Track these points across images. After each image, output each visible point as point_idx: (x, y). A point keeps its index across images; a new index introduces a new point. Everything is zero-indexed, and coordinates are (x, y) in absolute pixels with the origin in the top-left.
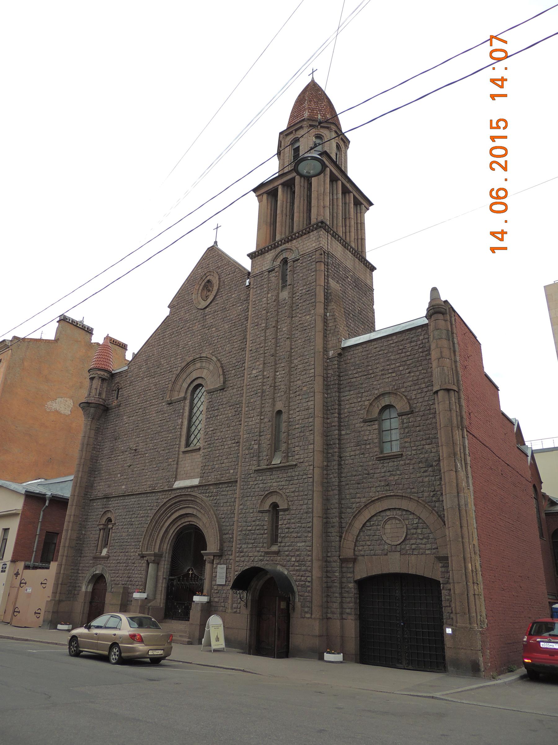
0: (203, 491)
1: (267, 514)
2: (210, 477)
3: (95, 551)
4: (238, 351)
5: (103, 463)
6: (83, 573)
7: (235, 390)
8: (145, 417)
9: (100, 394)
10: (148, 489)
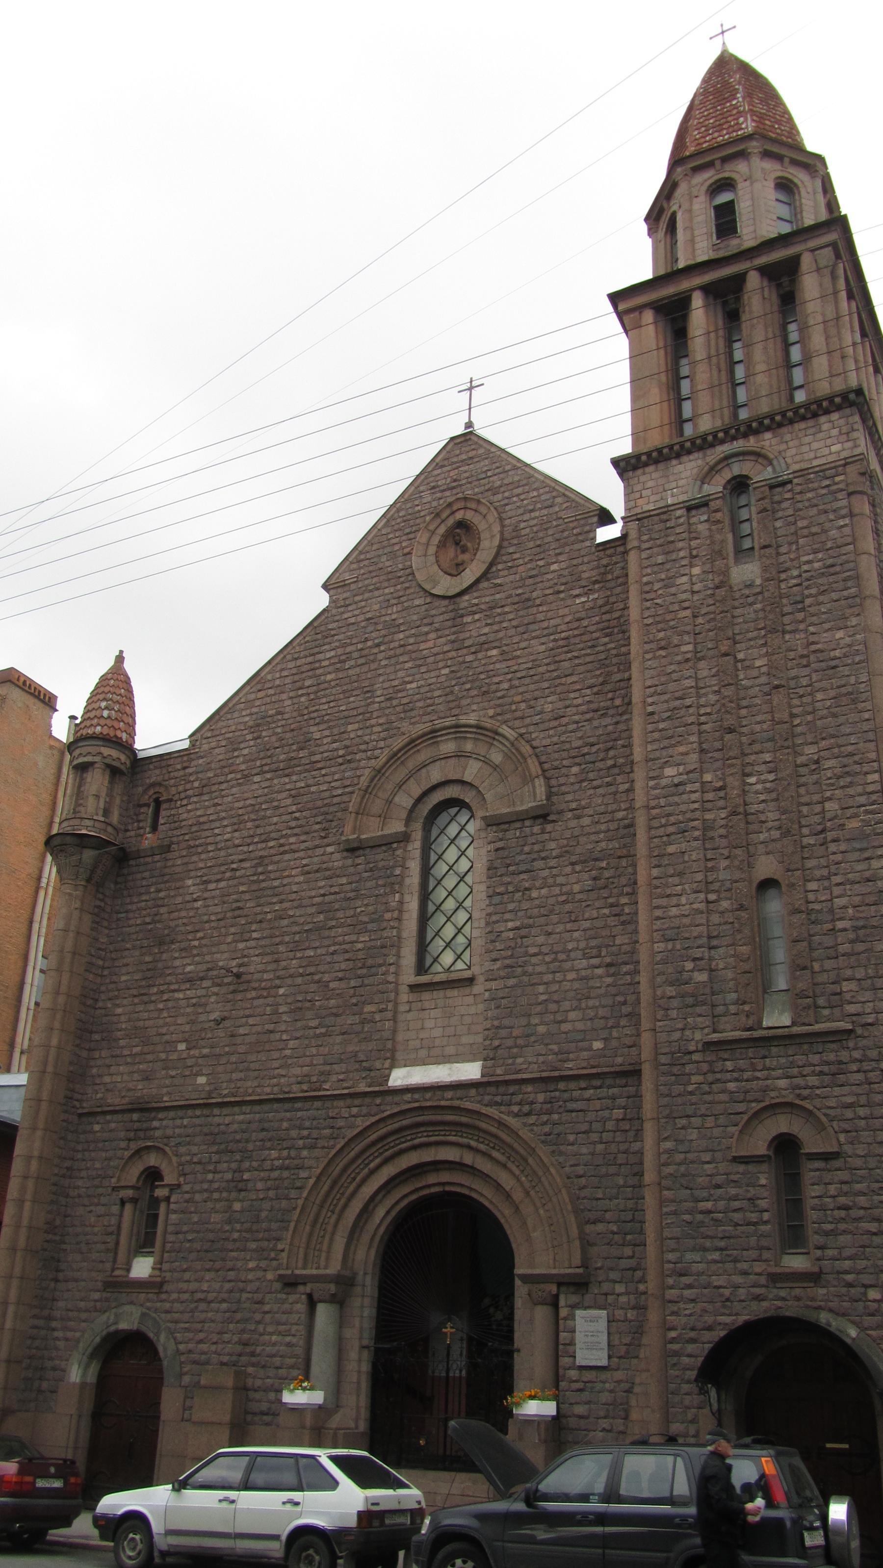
0: (498, 1099)
1: (765, 1167)
2: (519, 1060)
3: (108, 1266)
4: (588, 716)
5: (119, 1011)
6: (65, 1328)
7: (586, 821)
8: (264, 885)
9: (106, 812)
10: (295, 1088)
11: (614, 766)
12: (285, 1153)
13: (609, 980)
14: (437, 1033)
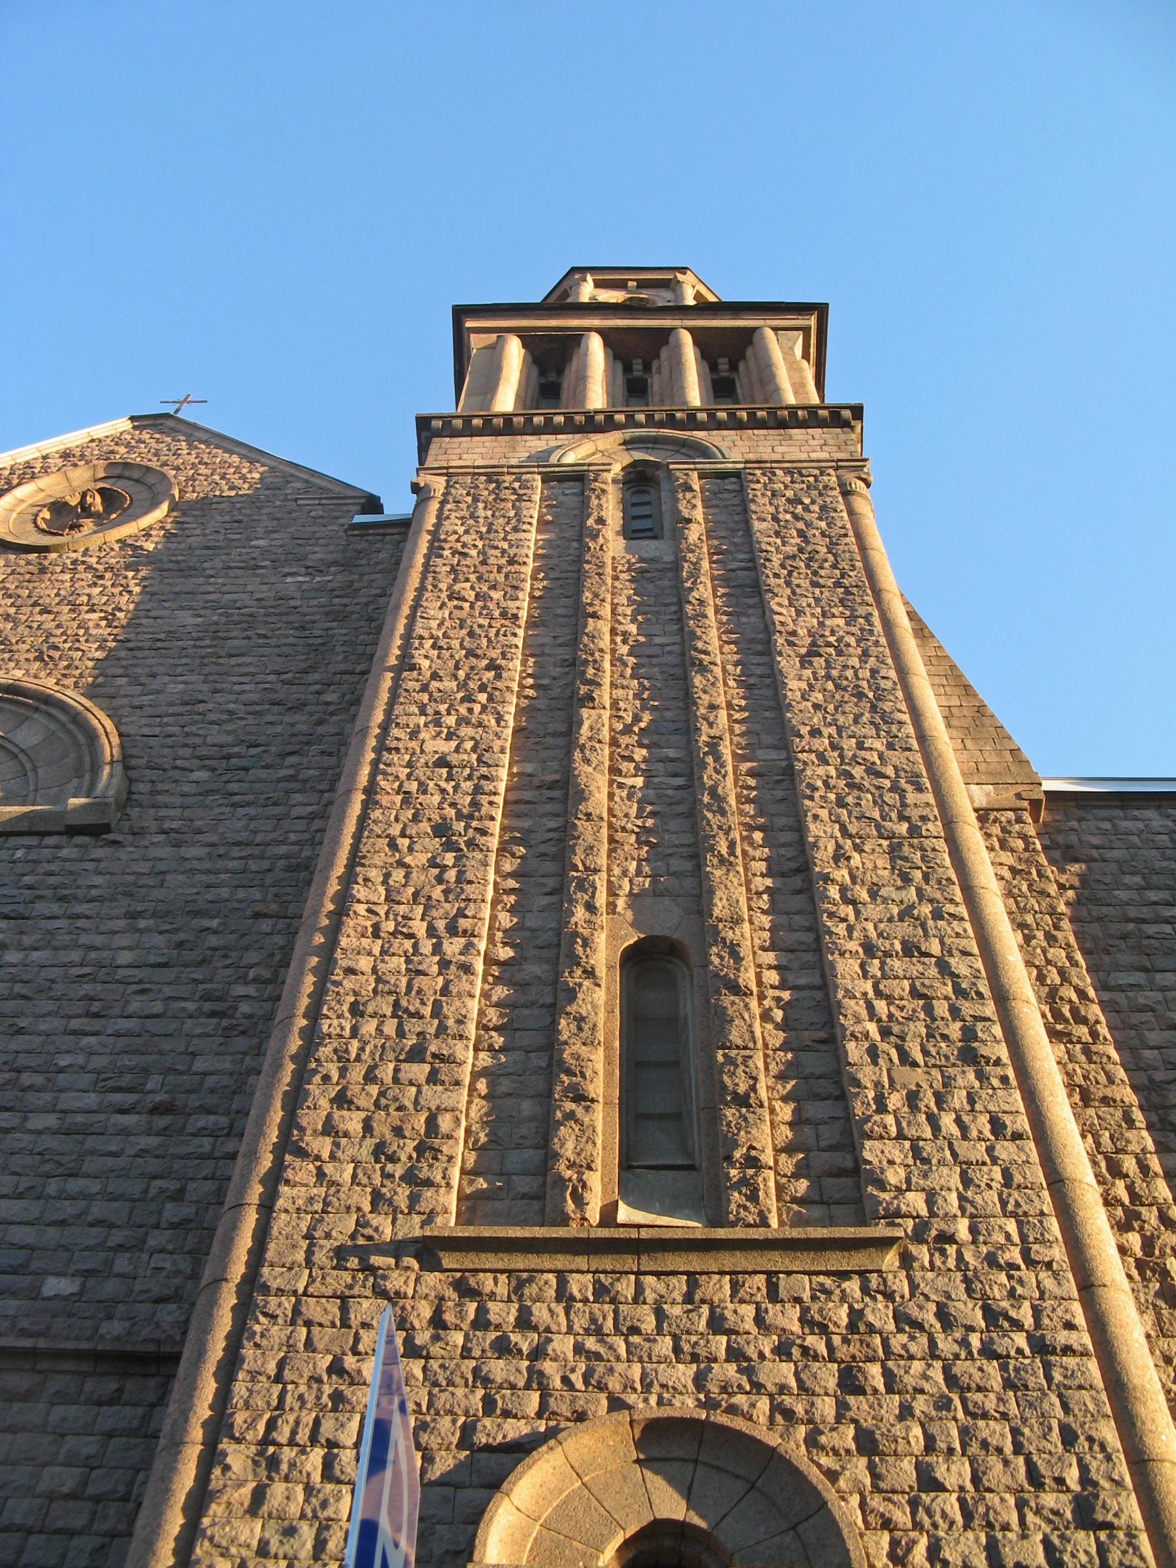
11: (293, 778)
13: (153, 1141)
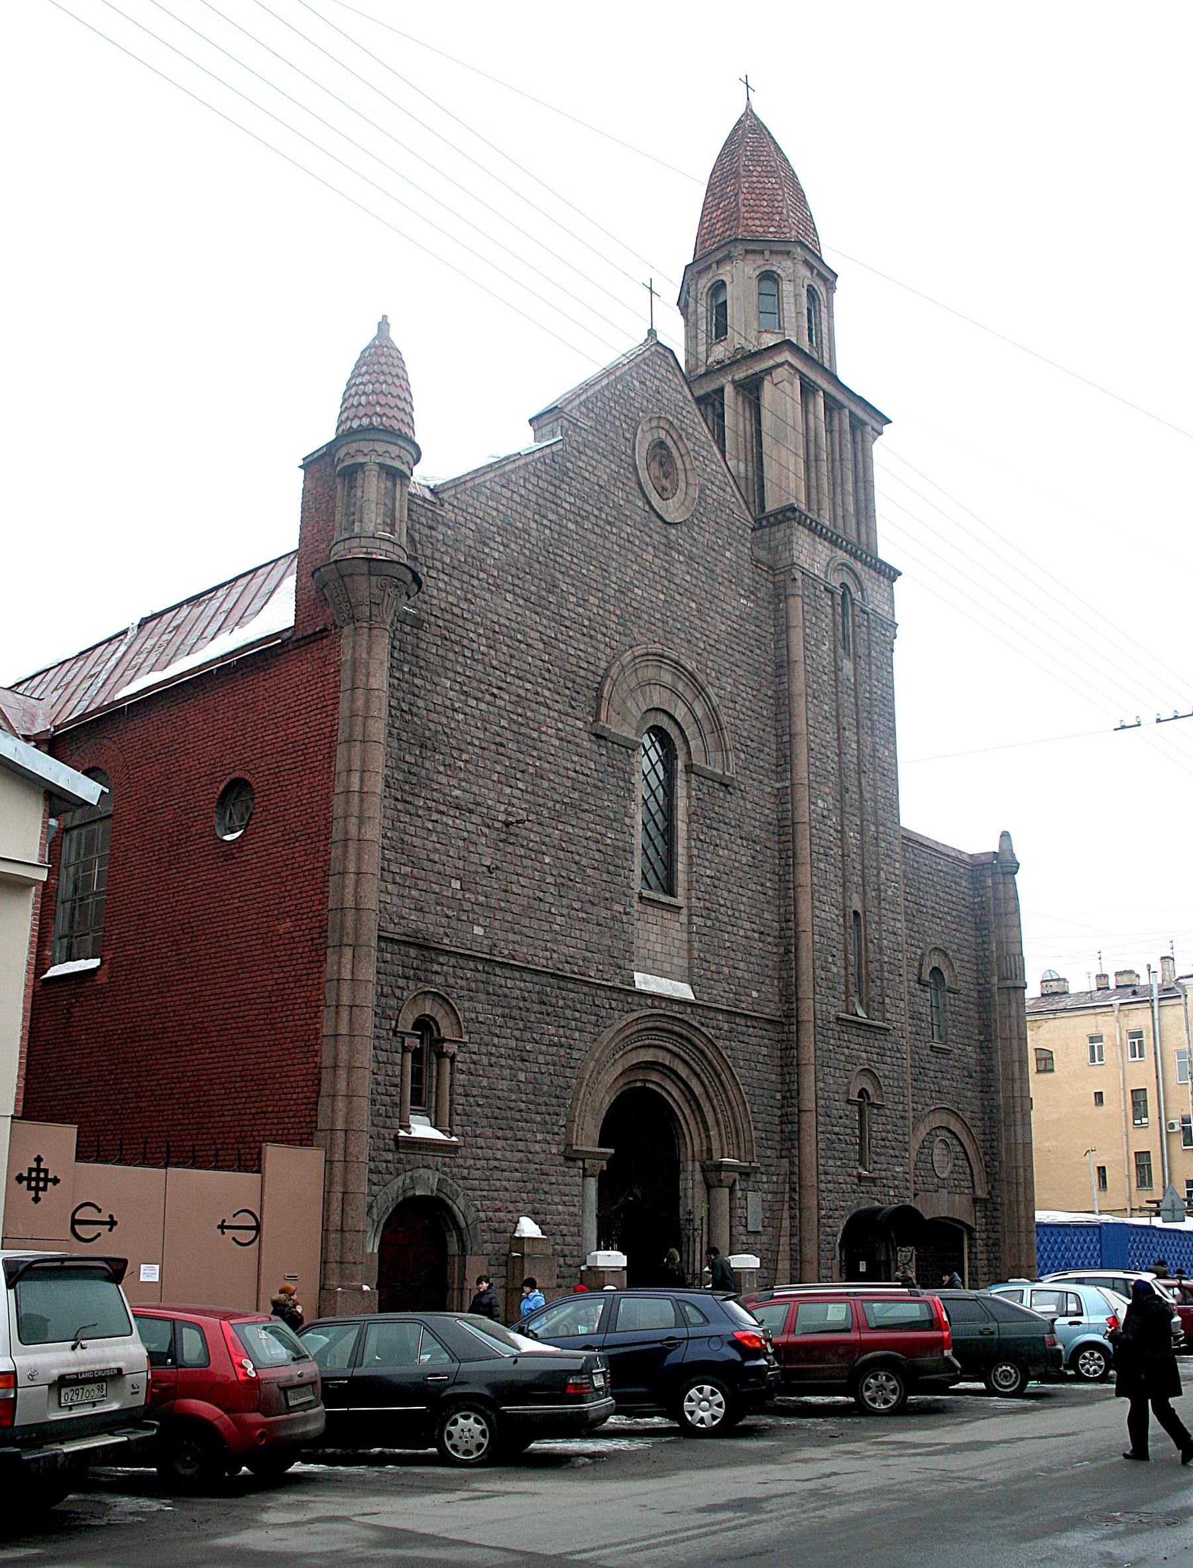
8: (523, 730)
12: (561, 1031)
14: (658, 948)
